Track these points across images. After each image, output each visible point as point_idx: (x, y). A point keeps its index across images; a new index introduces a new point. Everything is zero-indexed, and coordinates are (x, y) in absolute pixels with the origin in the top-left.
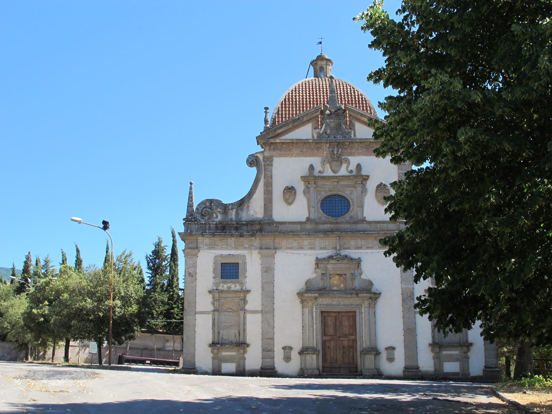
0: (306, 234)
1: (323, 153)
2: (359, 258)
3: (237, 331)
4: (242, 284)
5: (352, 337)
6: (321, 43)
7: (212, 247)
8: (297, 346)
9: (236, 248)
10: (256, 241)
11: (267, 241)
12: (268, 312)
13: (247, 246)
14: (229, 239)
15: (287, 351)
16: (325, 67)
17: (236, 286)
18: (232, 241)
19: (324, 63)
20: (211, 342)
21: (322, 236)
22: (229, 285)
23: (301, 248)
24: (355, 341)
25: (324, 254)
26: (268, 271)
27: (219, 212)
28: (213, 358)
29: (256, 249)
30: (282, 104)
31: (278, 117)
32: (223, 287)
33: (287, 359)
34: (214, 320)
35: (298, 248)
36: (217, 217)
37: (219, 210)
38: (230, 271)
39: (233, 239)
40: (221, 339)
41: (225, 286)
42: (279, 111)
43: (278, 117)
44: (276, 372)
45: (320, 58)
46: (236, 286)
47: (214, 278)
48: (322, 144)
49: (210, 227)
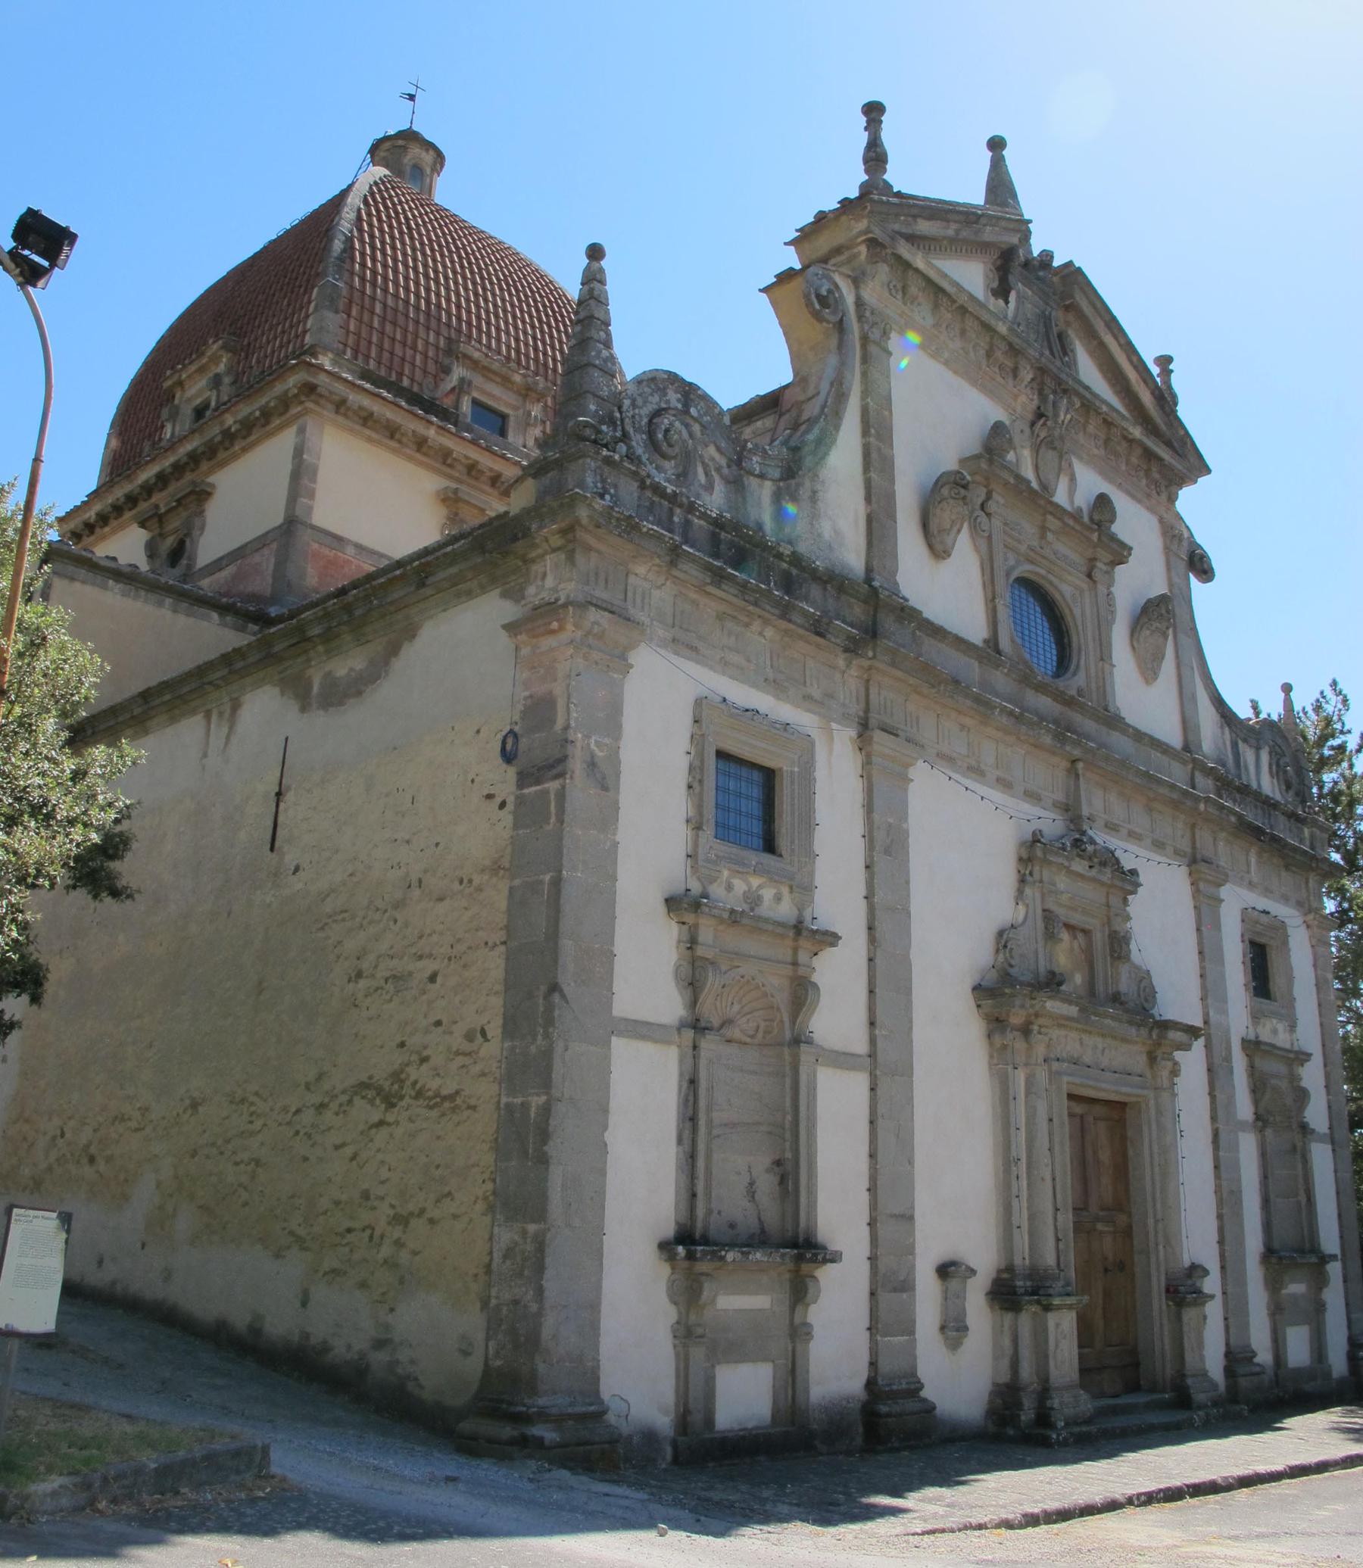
0: (1011, 713)
1: (1016, 397)
2: (1134, 872)
3: (762, 1162)
4: (804, 889)
5: (1122, 1219)
6: (412, 98)
7: (684, 643)
8: (984, 1260)
9: (776, 686)
10: (846, 680)
11: (892, 695)
12: (885, 1064)
13: (816, 693)
14: (756, 625)
15: (954, 1284)
16: (428, 171)
17: (778, 898)
18: (763, 637)
19: (428, 158)
20: (669, 1231)
21: (1048, 740)
22: (755, 882)
23: (976, 771)
24: (1128, 1233)
25: (1051, 823)
26: (885, 845)
27: (718, 470)
28: (686, 1334)
29: (845, 719)
30: (366, 202)
31: (362, 242)
32: (729, 888)
33: (953, 1329)
34: (691, 1083)
35: (970, 768)
36: (709, 487)
37: (712, 450)
38: (750, 801)
39: (769, 632)
40: (700, 1212)
41: (740, 886)
42: (359, 218)
43: (362, 242)
44: (929, 1409)
45: (409, 136)
46: (778, 898)
47: (696, 825)
48: (1023, 363)
49: (687, 523)
